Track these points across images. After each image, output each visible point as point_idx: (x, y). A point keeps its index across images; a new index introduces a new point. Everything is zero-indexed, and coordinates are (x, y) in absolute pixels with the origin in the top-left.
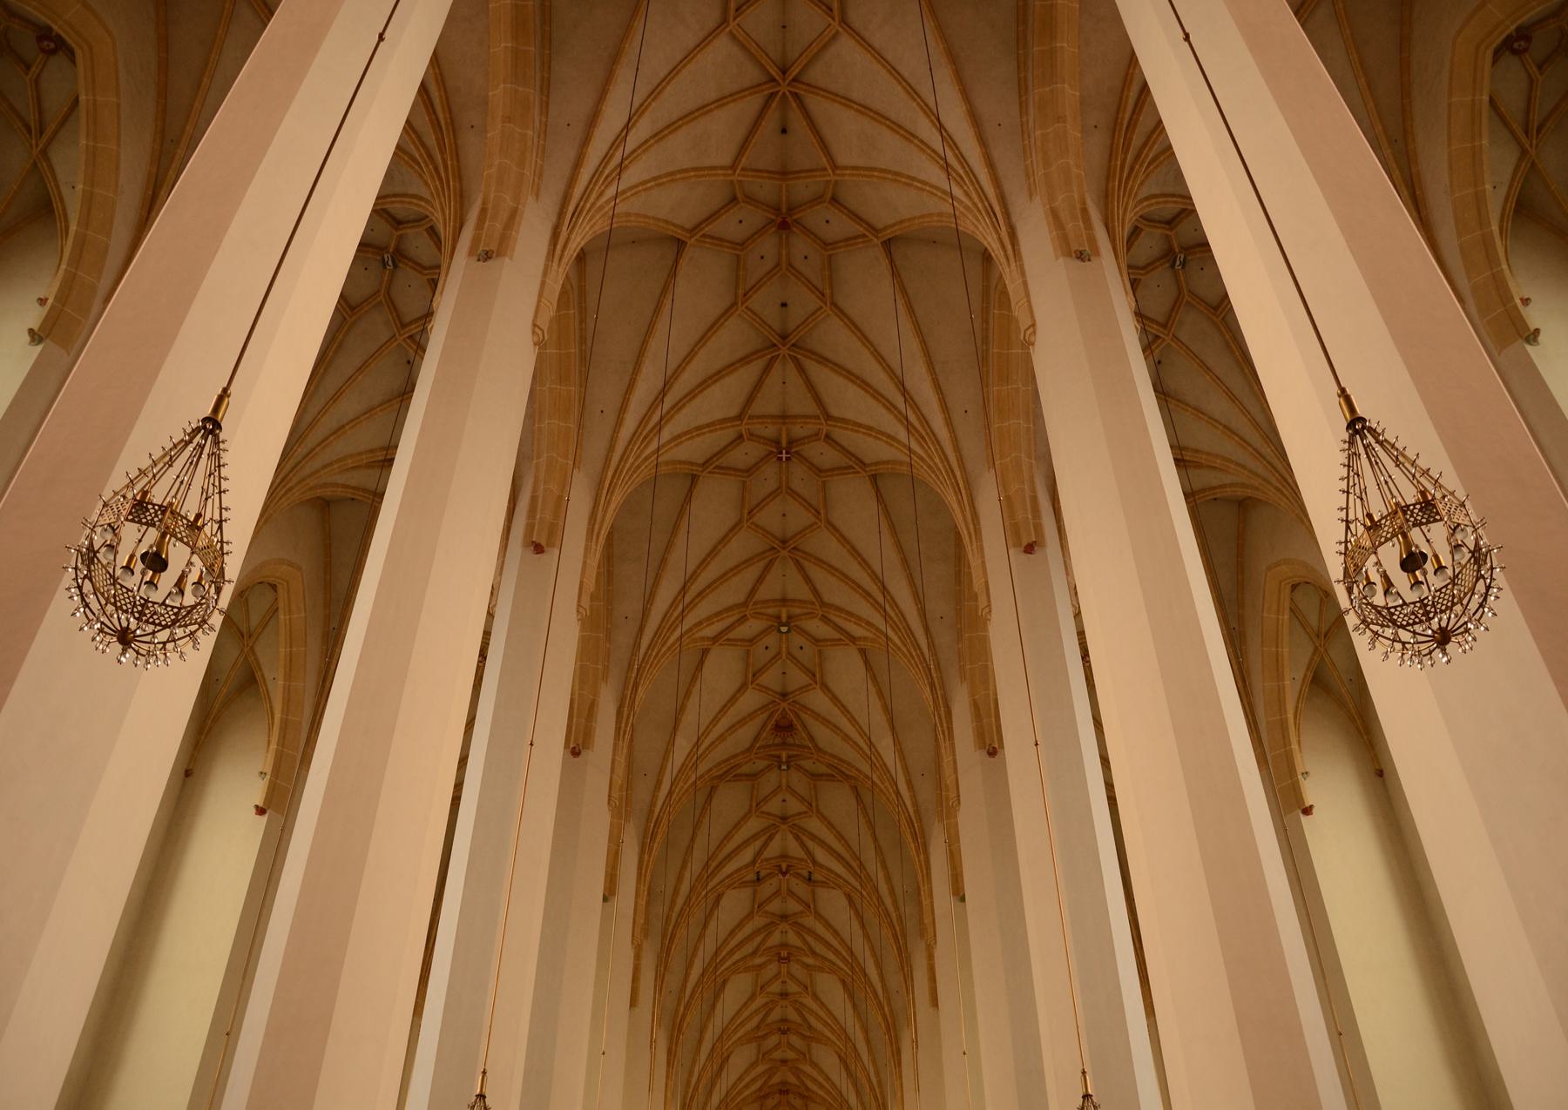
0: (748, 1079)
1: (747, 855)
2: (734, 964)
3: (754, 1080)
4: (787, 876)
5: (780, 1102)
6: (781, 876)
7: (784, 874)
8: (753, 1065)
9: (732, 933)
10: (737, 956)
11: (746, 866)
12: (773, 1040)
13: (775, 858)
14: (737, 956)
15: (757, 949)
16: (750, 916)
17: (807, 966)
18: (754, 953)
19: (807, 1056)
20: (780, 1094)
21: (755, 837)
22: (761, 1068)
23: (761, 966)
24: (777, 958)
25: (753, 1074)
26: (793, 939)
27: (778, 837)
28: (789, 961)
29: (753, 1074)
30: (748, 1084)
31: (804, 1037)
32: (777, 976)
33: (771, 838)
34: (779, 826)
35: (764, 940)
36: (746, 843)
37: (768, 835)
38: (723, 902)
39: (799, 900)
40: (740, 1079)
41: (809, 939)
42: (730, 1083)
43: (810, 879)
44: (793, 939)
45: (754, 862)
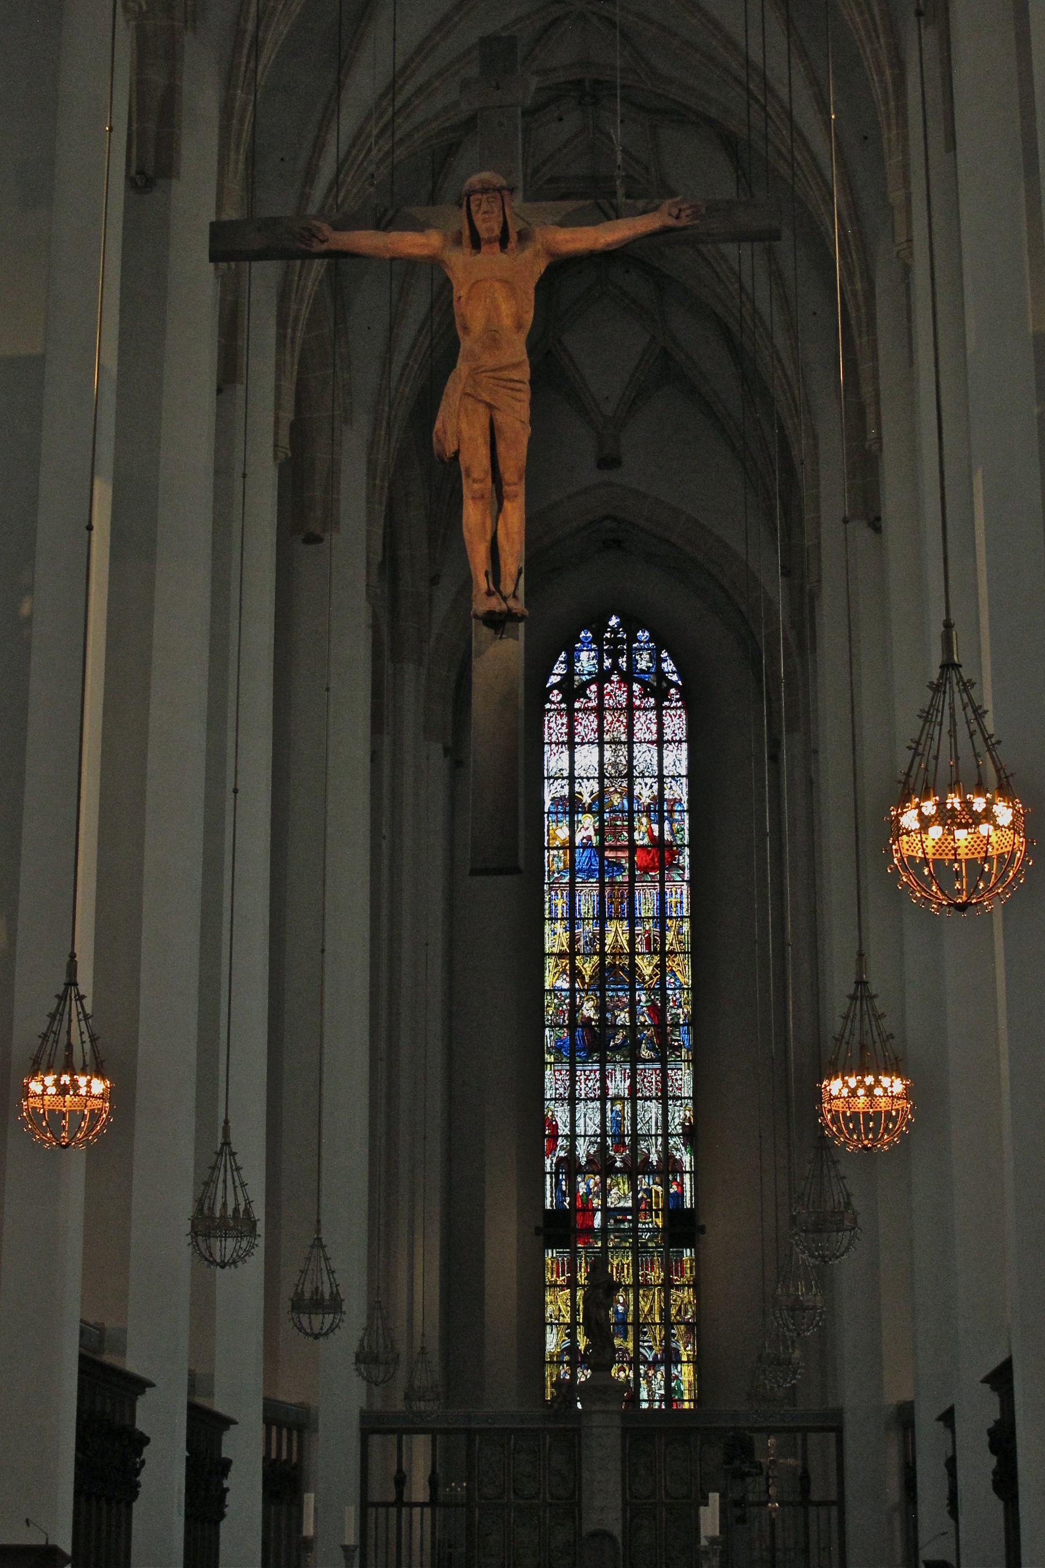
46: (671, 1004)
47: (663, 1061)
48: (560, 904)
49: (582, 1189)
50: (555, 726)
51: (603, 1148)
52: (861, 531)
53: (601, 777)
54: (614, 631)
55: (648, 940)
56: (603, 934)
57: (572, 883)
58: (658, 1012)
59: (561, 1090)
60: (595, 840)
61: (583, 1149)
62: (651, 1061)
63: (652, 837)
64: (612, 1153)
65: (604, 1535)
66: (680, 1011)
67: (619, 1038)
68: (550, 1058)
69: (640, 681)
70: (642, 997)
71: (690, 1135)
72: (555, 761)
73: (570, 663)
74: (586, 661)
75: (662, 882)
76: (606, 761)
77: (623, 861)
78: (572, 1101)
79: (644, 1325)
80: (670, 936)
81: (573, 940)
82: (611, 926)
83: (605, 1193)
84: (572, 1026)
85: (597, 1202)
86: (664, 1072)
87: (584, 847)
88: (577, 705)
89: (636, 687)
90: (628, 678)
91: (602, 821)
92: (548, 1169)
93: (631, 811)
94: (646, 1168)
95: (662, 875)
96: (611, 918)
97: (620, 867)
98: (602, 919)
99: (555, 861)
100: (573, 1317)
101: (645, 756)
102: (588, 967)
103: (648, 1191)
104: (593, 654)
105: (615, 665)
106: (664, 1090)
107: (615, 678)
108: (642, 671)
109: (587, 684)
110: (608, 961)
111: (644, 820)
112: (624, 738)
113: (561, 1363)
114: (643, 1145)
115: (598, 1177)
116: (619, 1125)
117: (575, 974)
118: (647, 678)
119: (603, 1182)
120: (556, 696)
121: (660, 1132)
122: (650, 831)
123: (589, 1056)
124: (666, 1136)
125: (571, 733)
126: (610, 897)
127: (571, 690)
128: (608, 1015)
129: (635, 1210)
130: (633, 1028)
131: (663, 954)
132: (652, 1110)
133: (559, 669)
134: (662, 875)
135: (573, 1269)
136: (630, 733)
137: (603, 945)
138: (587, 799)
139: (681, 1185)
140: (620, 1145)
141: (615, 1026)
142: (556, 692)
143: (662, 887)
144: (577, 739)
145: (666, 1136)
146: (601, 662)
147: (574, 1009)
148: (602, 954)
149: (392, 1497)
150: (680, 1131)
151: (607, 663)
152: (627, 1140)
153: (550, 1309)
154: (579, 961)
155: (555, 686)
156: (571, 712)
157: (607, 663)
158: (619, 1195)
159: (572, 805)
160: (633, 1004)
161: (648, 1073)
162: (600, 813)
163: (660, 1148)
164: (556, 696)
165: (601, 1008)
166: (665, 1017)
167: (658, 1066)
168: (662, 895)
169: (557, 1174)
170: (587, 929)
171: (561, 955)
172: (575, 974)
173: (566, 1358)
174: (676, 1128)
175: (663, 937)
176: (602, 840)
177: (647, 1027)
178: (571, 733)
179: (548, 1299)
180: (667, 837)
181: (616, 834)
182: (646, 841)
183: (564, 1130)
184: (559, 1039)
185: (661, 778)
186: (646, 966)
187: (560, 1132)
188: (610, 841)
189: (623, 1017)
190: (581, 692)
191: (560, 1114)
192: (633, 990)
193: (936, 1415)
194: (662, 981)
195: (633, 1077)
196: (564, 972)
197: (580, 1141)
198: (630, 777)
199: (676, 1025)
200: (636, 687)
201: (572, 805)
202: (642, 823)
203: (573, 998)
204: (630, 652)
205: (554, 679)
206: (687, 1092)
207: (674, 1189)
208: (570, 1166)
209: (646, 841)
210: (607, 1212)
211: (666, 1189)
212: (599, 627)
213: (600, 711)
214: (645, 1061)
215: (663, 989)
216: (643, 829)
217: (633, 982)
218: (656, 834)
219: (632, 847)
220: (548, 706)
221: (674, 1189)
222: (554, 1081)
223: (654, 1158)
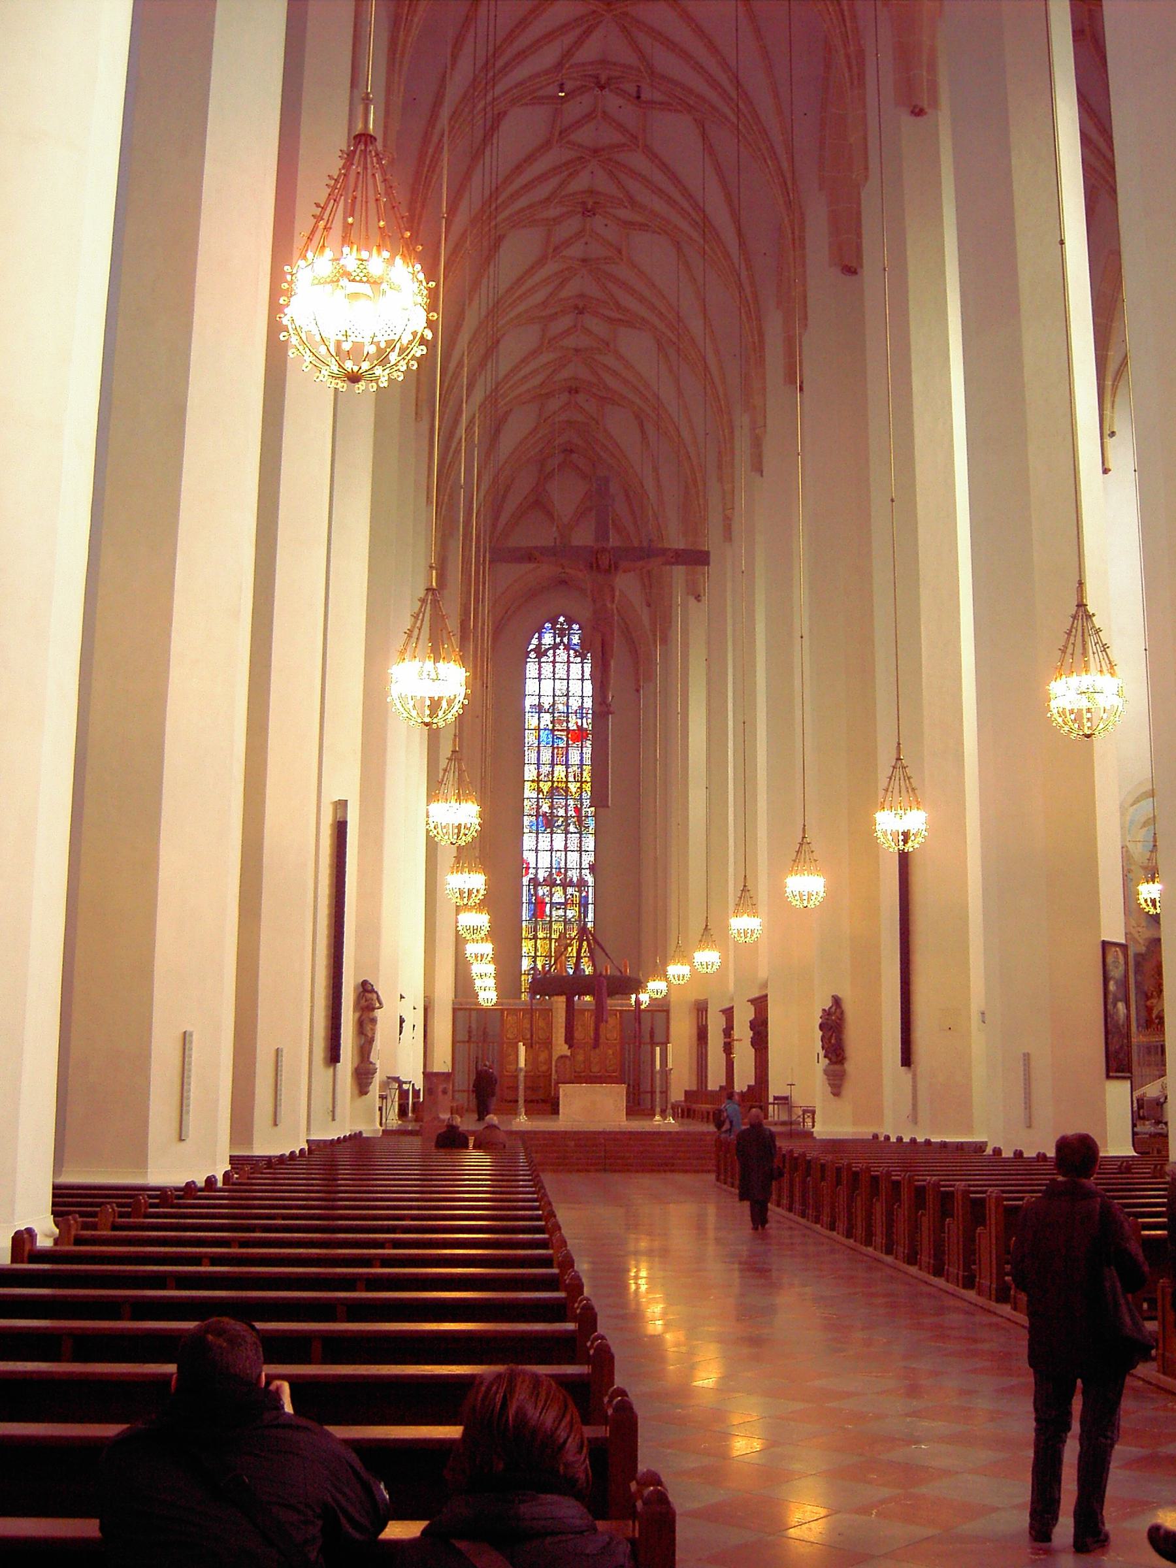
0: (526, 370)
1: (549, 56)
2: (517, 213)
3: (535, 372)
4: (606, 92)
5: (568, 403)
6: (597, 91)
7: (602, 88)
8: (534, 353)
9: (518, 169)
10: (522, 202)
11: (546, 72)
12: (566, 322)
13: (592, 63)
14: (522, 202)
15: (553, 194)
16: (546, 145)
17: (627, 224)
18: (548, 199)
19: (612, 346)
20: (570, 392)
21: (565, 28)
22: (547, 357)
23: (557, 221)
24: (580, 210)
25: (533, 366)
26: (603, 183)
27: (597, 35)
28: (594, 214)
29: (533, 366)
30: (525, 377)
31: (611, 320)
32: (579, 235)
33: (587, 33)
34: (602, 15)
35: (563, 184)
36: (549, 37)
37: (585, 26)
38: (505, 126)
39: (620, 127)
40: (516, 369)
41: (633, 186)
42: (502, 373)
43: (638, 97)
44: (603, 183)
45: (559, 65)
46: (585, 806)
47: (580, 833)
48: (534, 756)
49: (540, 893)
50: (531, 669)
51: (551, 874)
52: (692, 601)
53: (554, 696)
54: (562, 624)
55: (575, 775)
56: (553, 771)
57: (539, 747)
58: (578, 810)
59: (532, 846)
60: (550, 727)
61: (542, 875)
62: (575, 833)
63: (578, 726)
64: (555, 876)
65: (562, 1057)
66: (588, 810)
67: (559, 823)
68: (526, 830)
69: (573, 649)
70: (571, 802)
71: (592, 868)
72: (531, 686)
73: (540, 639)
74: (548, 639)
75: (582, 747)
76: (556, 688)
77: (564, 737)
78: (537, 851)
79: (569, 957)
80: (585, 774)
81: (539, 775)
82: (557, 768)
83: (551, 895)
84: (537, 816)
85: (547, 900)
86: (580, 838)
87: (545, 729)
88: (542, 660)
89: (572, 652)
90: (568, 647)
91: (554, 717)
92: (524, 883)
93: (568, 713)
94: (571, 884)
95: (582, 744)
96: (557, 764)
97: (562, 739)
98: (553, 765)
99: (530, 738)
100: (535, 953)
101: (575, 687)
102: (546, 787)
103: (572, 895)
104: (552, 635)
105: (562, 641)
106: (580, 847)
107: (562, 647)
108: (575, 645)
109: (549, 649)
110: (556, 784)
111: (574, 717)
112: (566, 677)
113: (528, 974)
114: (569, 873)
115: (548, 888)
116: (559, 863)
117: (539, 791)
118: (577, 648)
119: (551, 890)
120: (533, 655)
121: (578, 867)
122: (577, 723)
123: (545, 830)
124: (581, 869)
125: (540, 674)
126: (557, 754)
127: (540, 653)
128: (555, 811)
129: (565, 904)
130: (566, 818)
131: (582, 782)
132: (573, 858)
133: (535, 641)
134: (582, 744)
135: (535, 930)
136: (568, 675)
137: (553, 777)
138: (546, 706)
139: (587, 892)
140: (559, 874)
141: (557, 816)
142: (533, 653)
143: (582, 750)
144: (542, 677)
145: (581, 869)
146: (555, 640)
147: (539, 807)
148: (553, 782)
149: (466, 1039)
150: (587, 866)
151: (558, 640)
152: (563, 871)
153: (524, 950)
154: (541, 784)
155: (531, 650)
156: (540, 663)
157: (558, 640)
158: (558, 897)
159: (539, 709)
160: (567, 805)
161: (573, 839)
162: (553, 713)
163: (578, 875)
164: (533, 655)
165: (551, 807)
166: (582, 814)
167: (578, 835)
168: (582, 753)
169: (529, 885)
170: (545, 769)
171: (533, 781)
172: (539, 791)
173: (532, 972)
174: (585, 865)
175: (582, 774)
176: (554, 726)
177: (574, 817)
178: (540, 674)
179: (524, 944)
180: (585, 726)
181: (561, 722)
182: (575, 728)
183: (532, 865)
184: (531, 821)
185: (582, 697)
186: (573, 787)
187: (530, 866)
188: (558, 727)
189: (562, 812)
190: (545, 653)
191: (529, 856)
192: (567, 800)
193: (720, 1009)
194: (581, 795)
195: (566, 840)
196: (534, 789)
197: (539, 871)
198: (567, 695)
199: (587, 817)
200: (572, 652)
201: (539, 709)
202: (573, 719)
203: (538, 802)
204: (569, 634)
205: (532, 647)
206: (592, 848)
207: (584, 894)
208: (535, 882)
209: (575, 728)
210: (551, 903)
211: (581, 894)
212: (554, 622)
213: (554, 662)
214: (572, 833)
215: (581, 799)
216: (574, 721)
217: (566, 796)
218: (580, 724)
219: (568, 730)
220: (529, 660)
221: (584, 894)
222: (528, 841)
223: (575, 880)
